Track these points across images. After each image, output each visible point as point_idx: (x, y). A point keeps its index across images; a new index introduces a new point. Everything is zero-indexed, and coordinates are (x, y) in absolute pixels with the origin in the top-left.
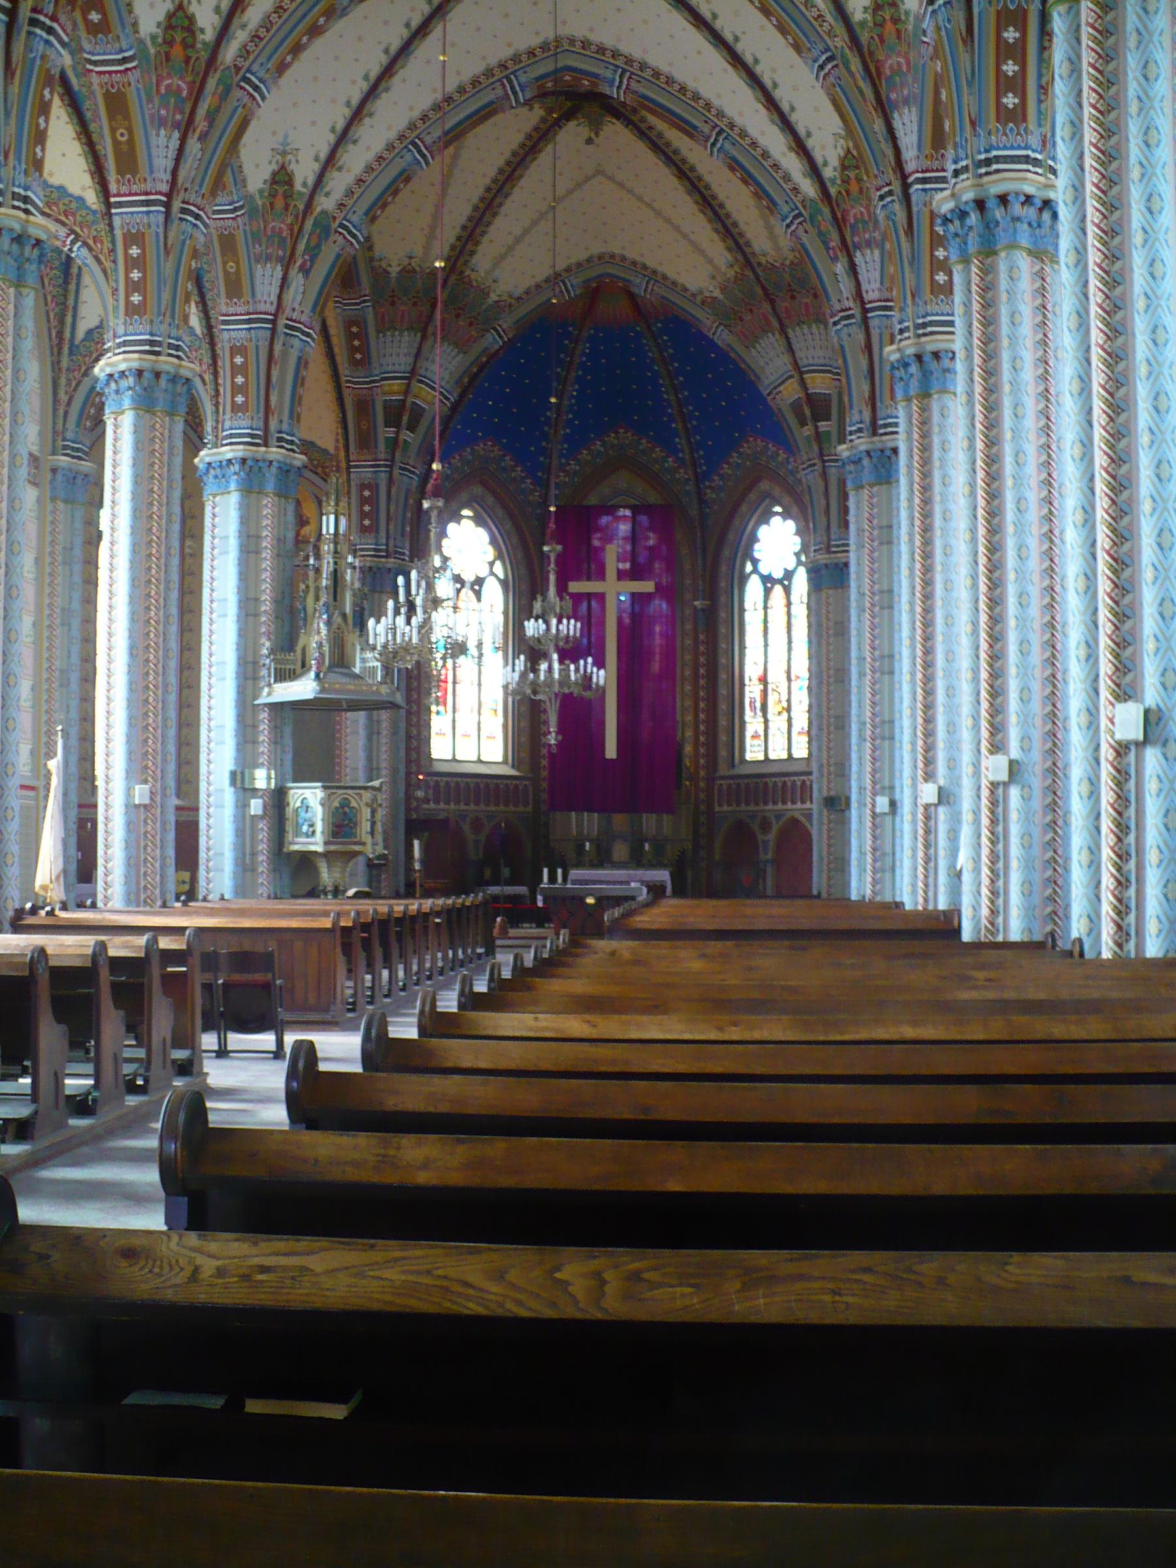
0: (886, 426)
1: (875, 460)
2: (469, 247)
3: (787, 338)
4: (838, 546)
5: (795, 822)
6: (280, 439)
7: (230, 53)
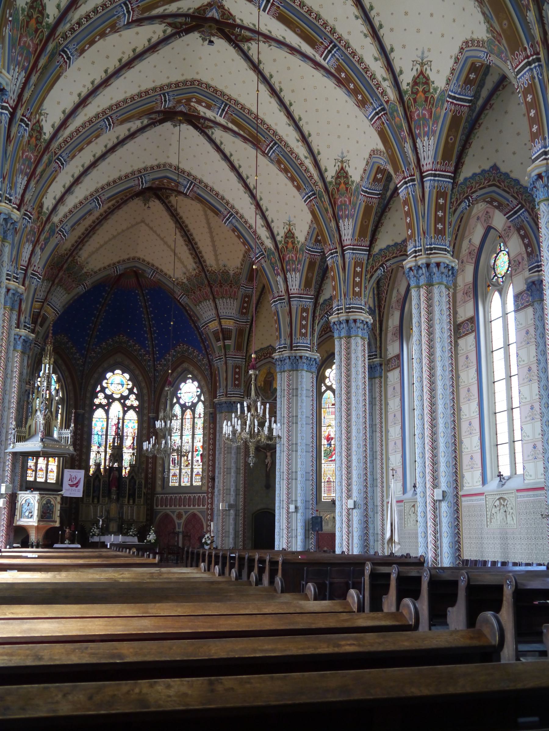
0: (297, 347)
1: (291, 360)
2: (80, 246)
3: (216, 304)
4: (231, 394)
5: (194, 515)
6: (25, 326)
7: (54, 145)
